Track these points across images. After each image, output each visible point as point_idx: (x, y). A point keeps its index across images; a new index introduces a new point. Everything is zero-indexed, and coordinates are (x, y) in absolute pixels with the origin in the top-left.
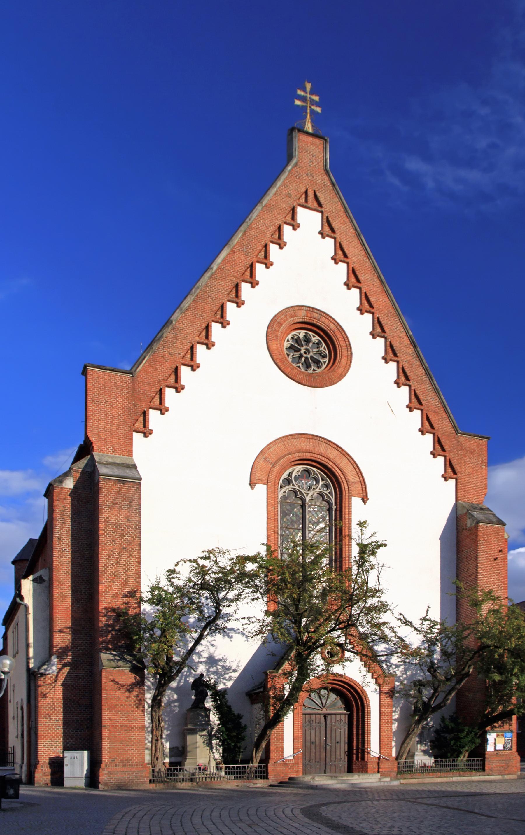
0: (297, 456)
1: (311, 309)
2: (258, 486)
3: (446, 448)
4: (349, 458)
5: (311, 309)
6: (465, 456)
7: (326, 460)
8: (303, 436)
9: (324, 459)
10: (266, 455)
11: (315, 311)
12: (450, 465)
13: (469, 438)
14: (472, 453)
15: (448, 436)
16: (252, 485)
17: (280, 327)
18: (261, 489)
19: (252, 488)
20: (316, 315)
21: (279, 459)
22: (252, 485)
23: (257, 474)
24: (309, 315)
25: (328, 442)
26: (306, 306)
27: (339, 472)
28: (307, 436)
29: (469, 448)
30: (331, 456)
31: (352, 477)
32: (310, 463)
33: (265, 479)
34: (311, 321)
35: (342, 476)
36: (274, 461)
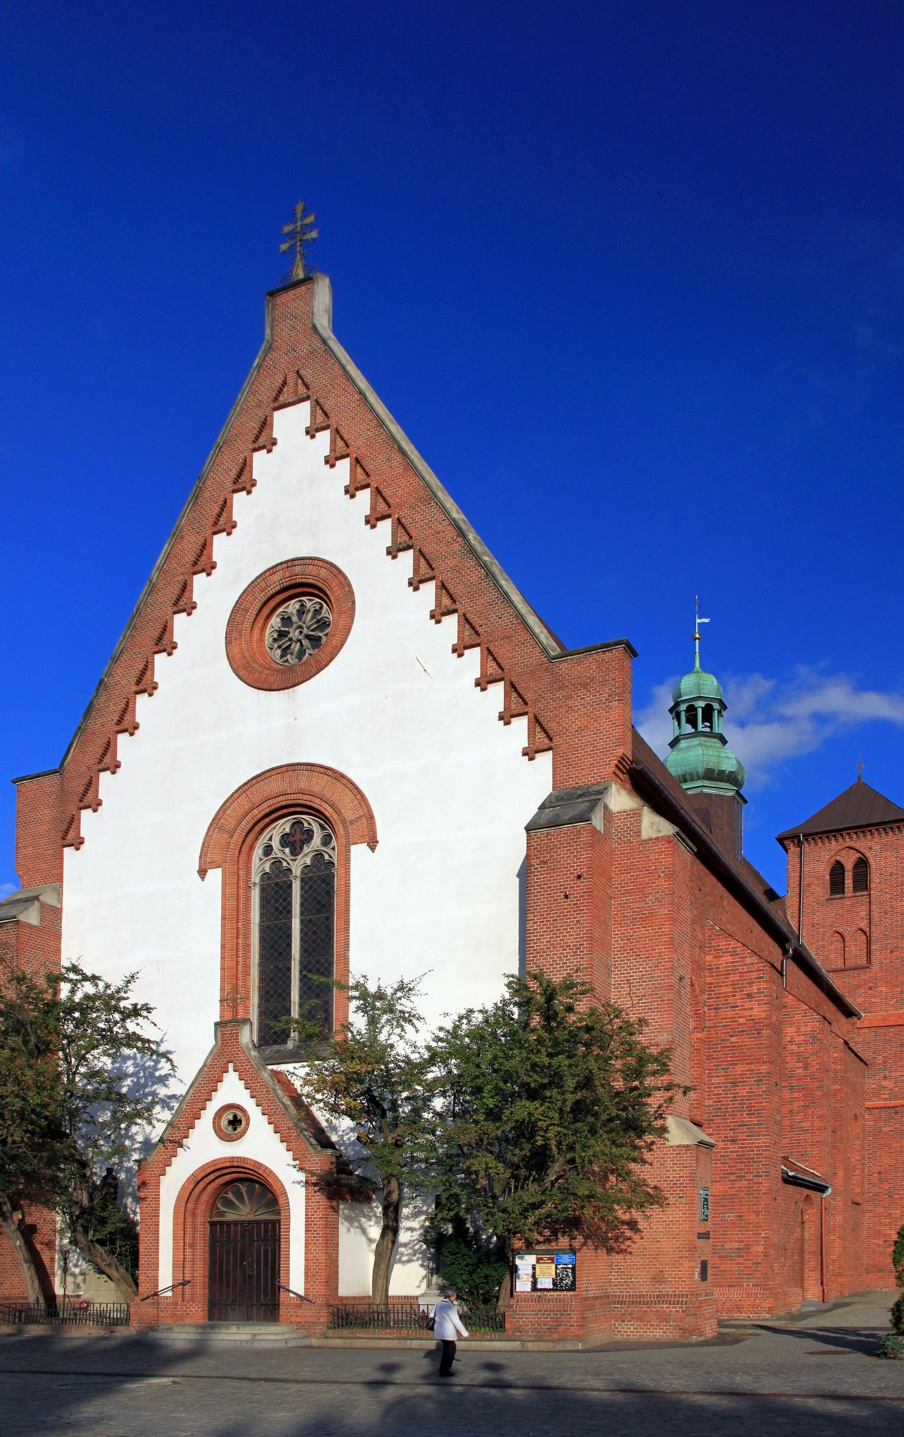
0: (266, 808)
1: (290, 564)
2: (210, 872)
3: (529, 696)
5: (290, 564)
6: (570, 697)
8: (273, 773)
9: (306, 797)
10: (222, 821)
13: (580, 658)
14: (585, 686)
15: (533, 672)
16: (202, 873)
18: (215, 876)
19: (203, 879)
20: (297, 569)
21: (239, 823)
22: (202, 873)
24: (288, 574)
25: (311, 767)
26: (281, 564)
29: (580, 677)
30: (317, 789)
32: (293, 809)
33: (218, 858)
34: (293, 582)
35: (335, 816)
36: (232, 826)
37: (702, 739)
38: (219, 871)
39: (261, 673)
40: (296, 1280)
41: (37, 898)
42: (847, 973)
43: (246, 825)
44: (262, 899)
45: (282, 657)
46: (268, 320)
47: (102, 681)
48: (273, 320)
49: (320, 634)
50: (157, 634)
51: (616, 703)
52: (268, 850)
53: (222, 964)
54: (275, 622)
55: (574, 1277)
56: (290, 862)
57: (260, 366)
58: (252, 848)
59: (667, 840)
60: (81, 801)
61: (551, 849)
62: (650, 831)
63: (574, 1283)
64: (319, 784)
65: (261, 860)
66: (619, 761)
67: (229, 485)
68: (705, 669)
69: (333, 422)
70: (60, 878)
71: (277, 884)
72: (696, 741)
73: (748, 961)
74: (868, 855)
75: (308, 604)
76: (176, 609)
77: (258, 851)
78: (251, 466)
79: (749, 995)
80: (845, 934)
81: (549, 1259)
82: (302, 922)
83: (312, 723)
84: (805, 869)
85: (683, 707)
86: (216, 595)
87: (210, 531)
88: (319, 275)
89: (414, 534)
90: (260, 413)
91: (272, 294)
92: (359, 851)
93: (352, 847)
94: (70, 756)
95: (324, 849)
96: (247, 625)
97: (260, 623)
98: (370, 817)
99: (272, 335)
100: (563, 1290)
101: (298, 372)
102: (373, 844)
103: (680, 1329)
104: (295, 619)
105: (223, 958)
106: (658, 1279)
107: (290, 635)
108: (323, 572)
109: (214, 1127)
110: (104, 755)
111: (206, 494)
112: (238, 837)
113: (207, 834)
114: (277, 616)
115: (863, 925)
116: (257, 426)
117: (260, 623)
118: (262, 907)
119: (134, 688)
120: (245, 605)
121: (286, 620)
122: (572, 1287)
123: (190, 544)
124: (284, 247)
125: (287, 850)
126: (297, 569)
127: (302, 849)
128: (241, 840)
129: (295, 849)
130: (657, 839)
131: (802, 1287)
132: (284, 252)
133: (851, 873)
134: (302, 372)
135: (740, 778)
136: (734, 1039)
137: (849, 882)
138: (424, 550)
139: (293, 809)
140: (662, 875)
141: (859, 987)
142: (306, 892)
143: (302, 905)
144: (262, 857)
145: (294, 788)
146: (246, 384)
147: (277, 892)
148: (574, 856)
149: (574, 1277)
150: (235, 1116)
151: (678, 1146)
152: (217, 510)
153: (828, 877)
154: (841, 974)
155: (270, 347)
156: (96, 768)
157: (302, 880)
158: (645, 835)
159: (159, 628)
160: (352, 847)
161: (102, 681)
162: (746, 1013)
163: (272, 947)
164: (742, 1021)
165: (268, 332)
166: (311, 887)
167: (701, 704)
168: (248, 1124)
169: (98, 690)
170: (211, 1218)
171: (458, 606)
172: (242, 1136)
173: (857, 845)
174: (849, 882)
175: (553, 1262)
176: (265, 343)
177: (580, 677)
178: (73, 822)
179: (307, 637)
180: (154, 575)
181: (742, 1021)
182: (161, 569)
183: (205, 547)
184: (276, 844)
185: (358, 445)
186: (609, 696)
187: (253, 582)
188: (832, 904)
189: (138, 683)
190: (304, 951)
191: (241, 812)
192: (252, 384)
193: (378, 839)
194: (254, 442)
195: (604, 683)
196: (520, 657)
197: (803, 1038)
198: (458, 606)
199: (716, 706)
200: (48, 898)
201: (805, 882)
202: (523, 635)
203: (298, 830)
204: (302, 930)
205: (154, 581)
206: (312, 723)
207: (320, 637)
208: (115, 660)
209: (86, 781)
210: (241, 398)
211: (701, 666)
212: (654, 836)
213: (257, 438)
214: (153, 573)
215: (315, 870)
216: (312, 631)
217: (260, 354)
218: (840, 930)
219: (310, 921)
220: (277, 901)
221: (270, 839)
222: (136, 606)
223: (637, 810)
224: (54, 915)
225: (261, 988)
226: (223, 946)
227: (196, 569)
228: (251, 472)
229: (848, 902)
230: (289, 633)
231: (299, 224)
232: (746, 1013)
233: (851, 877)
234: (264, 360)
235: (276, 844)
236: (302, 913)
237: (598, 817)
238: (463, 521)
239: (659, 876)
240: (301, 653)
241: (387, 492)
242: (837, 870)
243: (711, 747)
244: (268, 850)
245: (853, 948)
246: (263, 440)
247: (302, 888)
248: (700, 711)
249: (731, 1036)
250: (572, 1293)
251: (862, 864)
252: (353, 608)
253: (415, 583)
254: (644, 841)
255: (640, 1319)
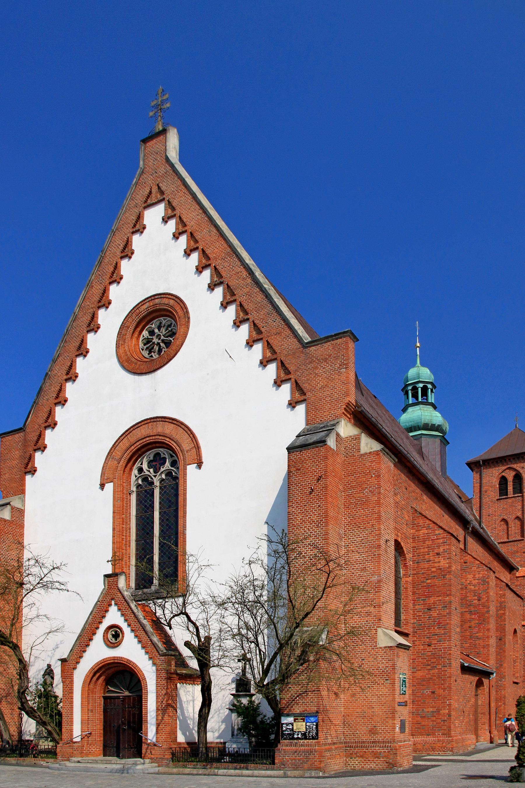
1: (153, 298)
3: (291, 368)
4: (183, 427)
5: (153, 298)
6: (316, 368)
7: (163, 438)
9: (161, 438)
11: (156, 297)
12: (298, 387)
14: (326, 360)
15: (294, 353)
16: (102, 486)
17: (127, 330)
18: (109, 487)
19: (102, 489)
20: (157, 301)
22: (102, 486)
23: (106, 475)
25: (164, 419)
27: (175, 445)
28: (146, 422)
29: (322, 355)
31: (186, 445)
33: (111, 476)
35: (178, 448)
37: (421, 406)
38: (111, 484)
39: (136, 364)
40: (151, 733)
41: (9, 504)
42: (510, 544)
43: (127, 456)
44: (137, 500)
45: (149, 354)
46: (142, 156)
47: (47, 374)
48: (145, 156)
49: (171, 339)
50: (78, 344)
51: (345, 370)
52: (140, 470)
53: (113, 540)
54: (145, 333)
55: (317, 731)
56: (153, 477)
57: (136, 183)
58: (131, 469)
59: (377, 453)
60: (35, 446)
61: (302, 461)
62: (366, 448)
63: (317, 734)
64: (169, 429)
65: (136, 476)
66: (346, 406)
67: (119, 254)
68: (423, 364)
69: (177, 212)
70: (23, 492)
71: (146, 491)
72: (417, 408)
73: (437, 532)
74: (521, 472)
75: (164, 322)
76: (88, 329)
77: (135, 472)
78: (132, 242)
79: (438, 554)
80: (509, 520)
81: (301, 719)
82: (160, 513)
83: (165, 393)
84: (484, 481)
85: (410, 388)
86: (111, 320)
87: (108, 282)
88: (170, 128)
89: (223, 274)
90: (137, 211)
91: (145, 141)
92: (191, 469)
93: (188, 467)
94: (29, 419)
95: (173, 468)
96: (128, 336)
97: (137, 333)
98: (197, 447)
99: (144, 164)
100: (310, 739)
101: (158, 185)
102: (200, 465)
103: (387, 763)
104: (156, 331)
105: (113, 537)
106: (373, 731)
107: (153, 341)
108: (172, 302)
109: (104, 639)
110: (48, 418)
111: (106, 260)
112: (123, 463)
113: (105, 462)
114: (146, 330)
115: (519, 514)
116: (135, 218)
117: (136, 335)
118: (137, 505)
119: (65, 377)
120: (127, 324)
121: (152, 333)
122: (316, 737)
123: (97, 290)
124: (151, 114)
125: (152, 470)
126: (157, 301)
127: (160, 469)
128: (124, 465)
129: (156, 469)
130: (370, 453)
131: (477, 736)
132: (151, 117)
133: (511, 483)
134: (161, 185)
135: (444, 429)
136: (429, 581)
137: (510, 488)
138: (230, 284)
139: (154, 445)
140: (373, 476)
141: (517, 552)
142: (163, 495)
143: (160, 503)
144: (137, 474)
145: (155, 432)
146: (128, 194)
147: (146, 496)
148: (317, 465)
149: (317, 731)
150: (116, 632)
151: (385, 647)
152: (112, 269)
153: (498, 486)
154: (506, 544)
155: (143, 172)
156: (43, 426)
157: (160, 488)
158: (362, 451)
159: (79, 340)
160: (188, 467)
161: (47, 374)
162: (436, 565)
163: (143, 529)
164: (434, 569)
165: (141, 163)
166: (165, 492)
167: (421, 385)
168: (123, 637)
169: (45, 379)
170: (104, 694)
171: (249, 316)
172: (120, 644)
173: (514, 466)
174: (510, 488)
175: (304, 721)
176: (139, 170)
177: (322, 355)
178: (31, 459)
179: (163, 341)
180: (77, 310)
181: (434, 569)
182: (80, 306)
183: (105, 291)
184: (145, 466)
185: (191, 225)
186: (340, 365)
187: (131, 310)
188: (500, 502)
189: (67, 374)
190: (161, 531)
191: (124, 448)
192: (132, 194)
193: (203, 461)
194: (133, 228)
195: (336, 358)
196: (285, 345)
197: (477, 581)
198: (249, 316)
199: (429, 386)
200: (16, 503)
201: (483, 489)
202: (288, 332)
203: (158, 458)
204: (160, 519)
205: (76, 313)
206: (165, 393)
207: (171, 340)
208: (54, 361)
209: (38, 434)
210: (126, 202)
211: (421, 363)
212: (368, 452)
213: (135, 226)
214: (76, 308)
215: (167, 482)
216: (167, 337)
217: (136, 176)
218: (506, 518)
219: (165, 512)
220: (146, 501)
221: (142, 464)
222: (67, 328)
223: (358, 435)
224: (19, 513)
225: (137, 555)
226: (114, 529)
227: (100, 304)
228: (131, 245)
229: (510, 501)
230: (153, 339)
231: (160, 100)
232: (436, 565)
233: (511, 485)
234: (139, 179)
235: (145, 466)
236: (160, 508)
237: (332, 440)
238: (253, 265)
239: (372, 477)
240: (160, 351)
241: (208, 251)
242: (503, 481)
243: (427, 410)
244: (140, 470)
245: (513, 528)
246: (139, 227)
247: (160, 493)
248: (420, 390)
249: (428, 579)
250: (316, 741)
251: (518, 477)
252: (189, 322)
253: (225, 304)
254: (362, 455)
255: (362, 756)
